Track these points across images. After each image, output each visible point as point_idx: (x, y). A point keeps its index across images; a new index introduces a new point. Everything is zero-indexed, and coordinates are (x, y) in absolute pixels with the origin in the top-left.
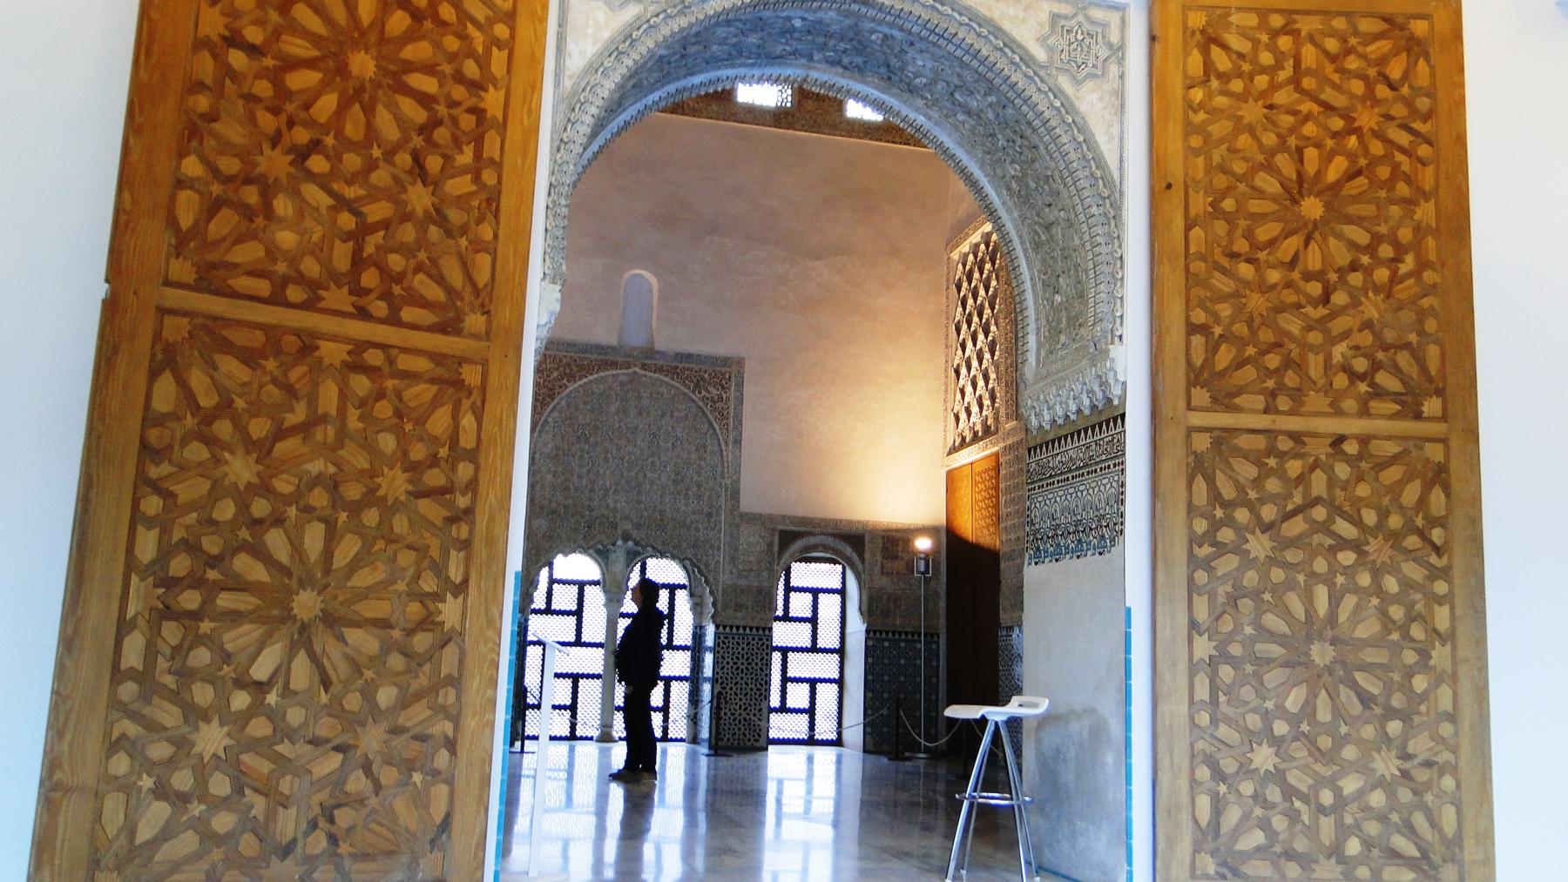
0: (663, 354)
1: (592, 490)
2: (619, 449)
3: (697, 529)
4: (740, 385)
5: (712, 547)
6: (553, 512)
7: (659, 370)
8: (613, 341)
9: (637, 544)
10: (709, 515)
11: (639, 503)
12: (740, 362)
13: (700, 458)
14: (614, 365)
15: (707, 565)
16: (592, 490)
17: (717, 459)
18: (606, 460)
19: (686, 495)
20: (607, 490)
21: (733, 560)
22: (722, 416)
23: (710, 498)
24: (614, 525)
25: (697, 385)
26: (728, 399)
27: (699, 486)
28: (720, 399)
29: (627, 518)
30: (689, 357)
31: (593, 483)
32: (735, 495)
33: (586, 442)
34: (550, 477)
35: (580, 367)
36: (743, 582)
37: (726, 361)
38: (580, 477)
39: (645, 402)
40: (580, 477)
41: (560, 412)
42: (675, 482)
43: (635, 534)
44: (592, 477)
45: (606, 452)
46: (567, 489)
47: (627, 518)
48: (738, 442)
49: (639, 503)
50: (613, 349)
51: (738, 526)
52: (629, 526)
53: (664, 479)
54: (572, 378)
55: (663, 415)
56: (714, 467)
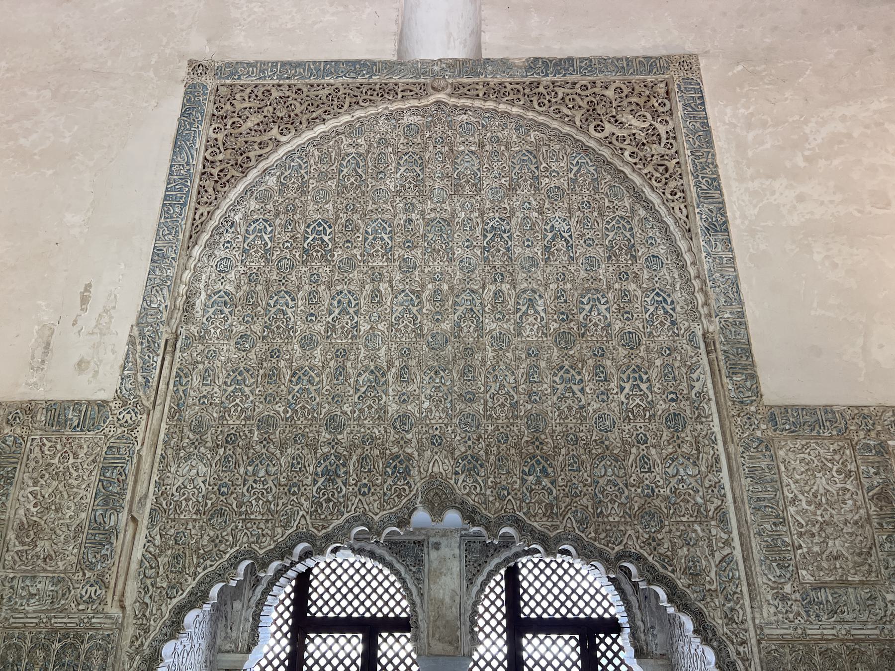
0: (504, 64)
1: (341, 371)
2: (408, 267)
3: (644, 462)
4: (697, 106)
5: (700, 514)
6: (230, 439)
7: (498, 92)
8: (387, 52)
9: (470, 515)
10: (674, 420)
11: (469, 398)
12: (687, 62)
13: (623, 276)
14: (387, 92)
15: (695, 575)
16: (341, 371)
17: (668, 274)
18: (376, 297)
19: (599, 369)
20: (379, 373)
21: (777, 553)
22: (665, 172)
23: (667, 371)
24: (401, 467)
25: (592, 114)
26: (672, 135)
27: (631, 342)
28: (654, 136)
29: (436, 442)
30: (565, 64)
31: (342, 354)
32: (739, 359)
33: (326, 259)
34: (228, 350)
35: (312, 104)
36: (823, 628)
37: (650, 64)
38: (308, 342)
39: (468, 165)
40: (308, 342)
41: (264, 198)
42: (565, 340)
43: (461, 486)
44: (340, 341)
45: (376, 277)
46: (273, 375)
47: (436, 442)
48: (719, 227)
49: (469, 398)
50: (389, 67)
51: (767, 445)
52: (442, 466)
53: (530, 333)
54: (290, 124)
55: (513, 189)
56: (662, 297)
